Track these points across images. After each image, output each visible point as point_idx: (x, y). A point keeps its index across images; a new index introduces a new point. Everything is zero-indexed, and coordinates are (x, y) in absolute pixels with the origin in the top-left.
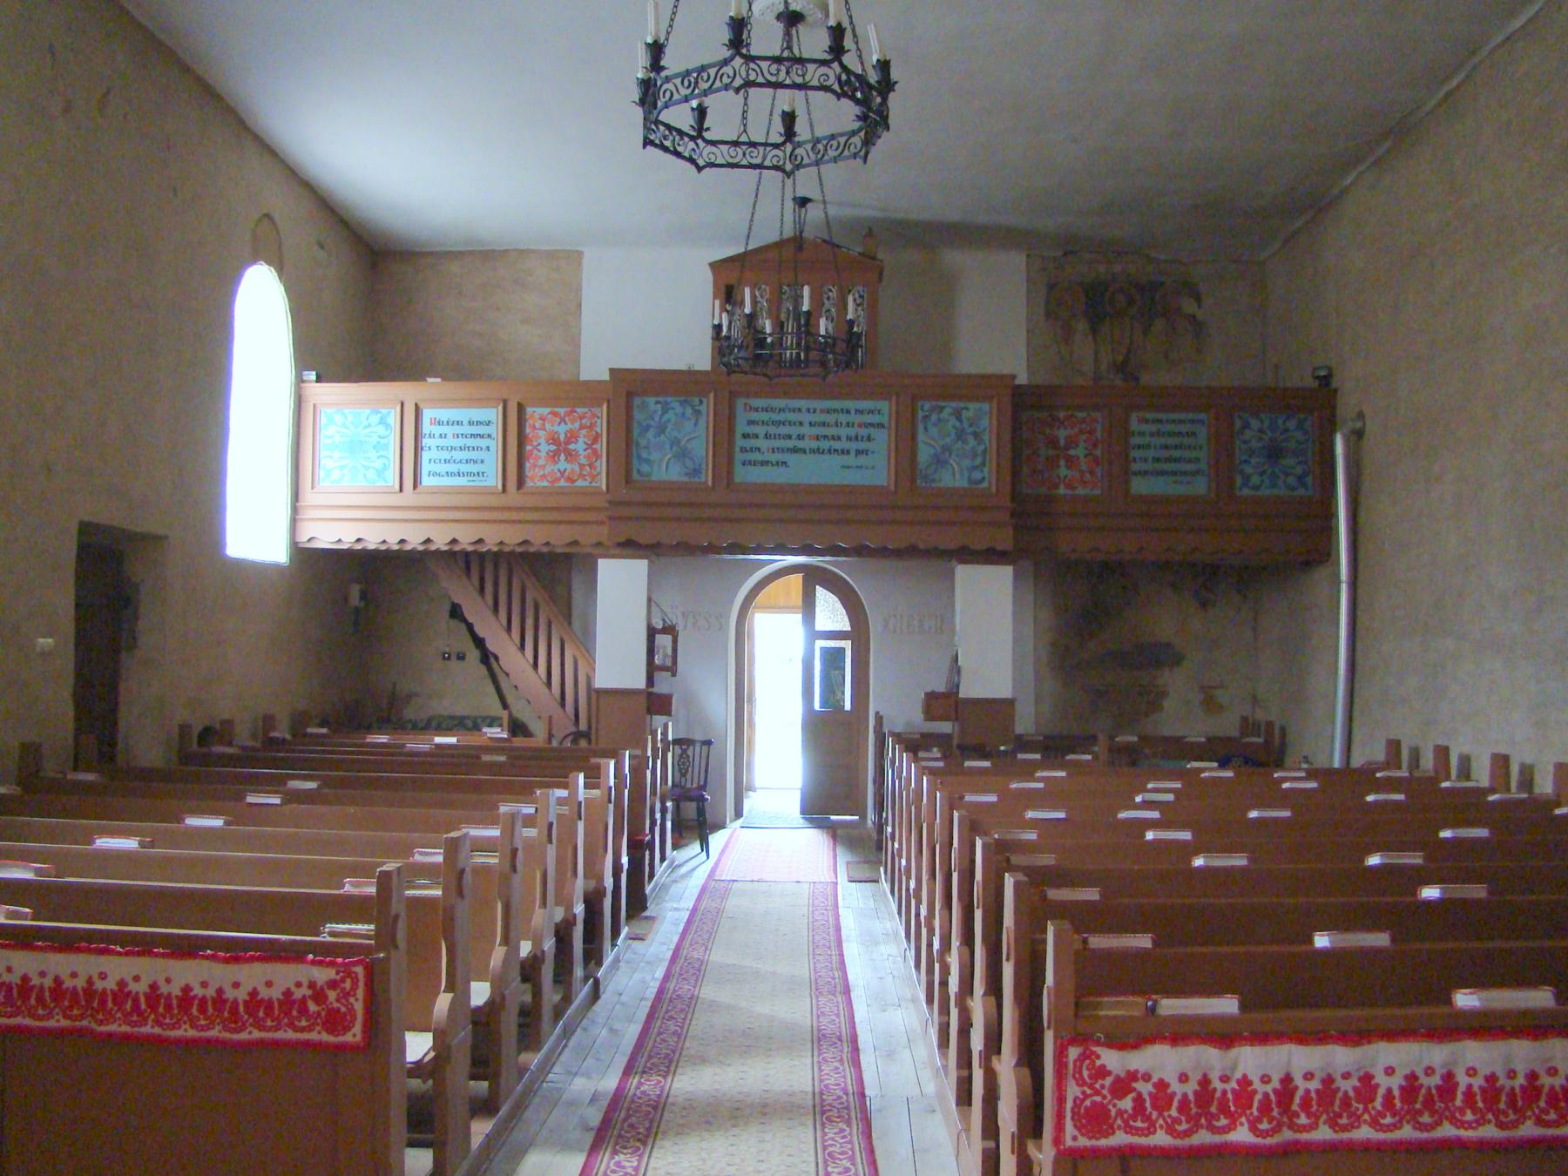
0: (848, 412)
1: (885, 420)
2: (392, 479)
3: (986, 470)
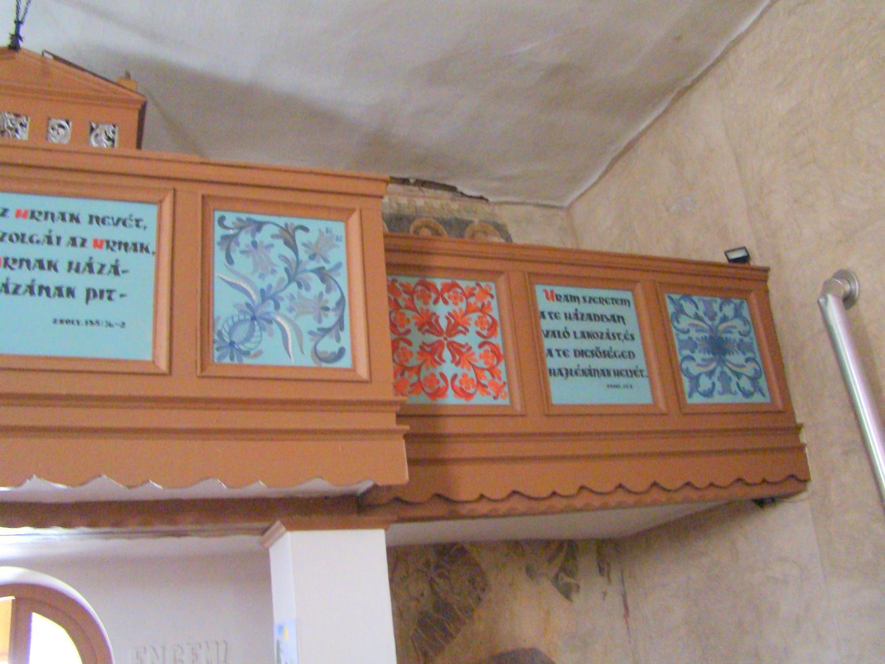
0: (75, 218)
1: (148, 237)
3: (345, 335)
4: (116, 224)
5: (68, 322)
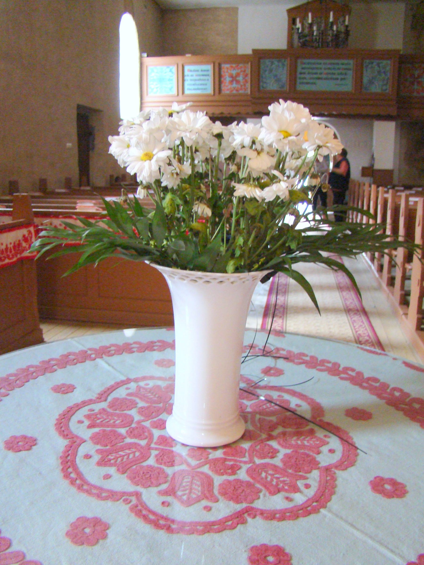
0: (338, 64)
1: (351, 67)
2: (175, 92)
3: (388, 86)
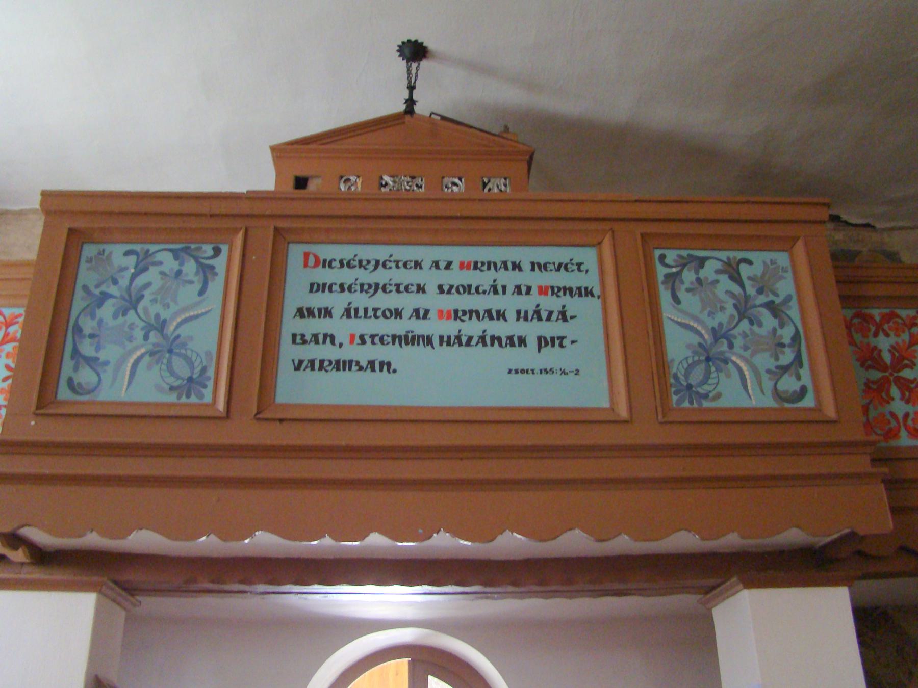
0: (517, 266)
1: (591, 280)
3: (805, 372)
4: (558, 269)
5: (523, 371)
